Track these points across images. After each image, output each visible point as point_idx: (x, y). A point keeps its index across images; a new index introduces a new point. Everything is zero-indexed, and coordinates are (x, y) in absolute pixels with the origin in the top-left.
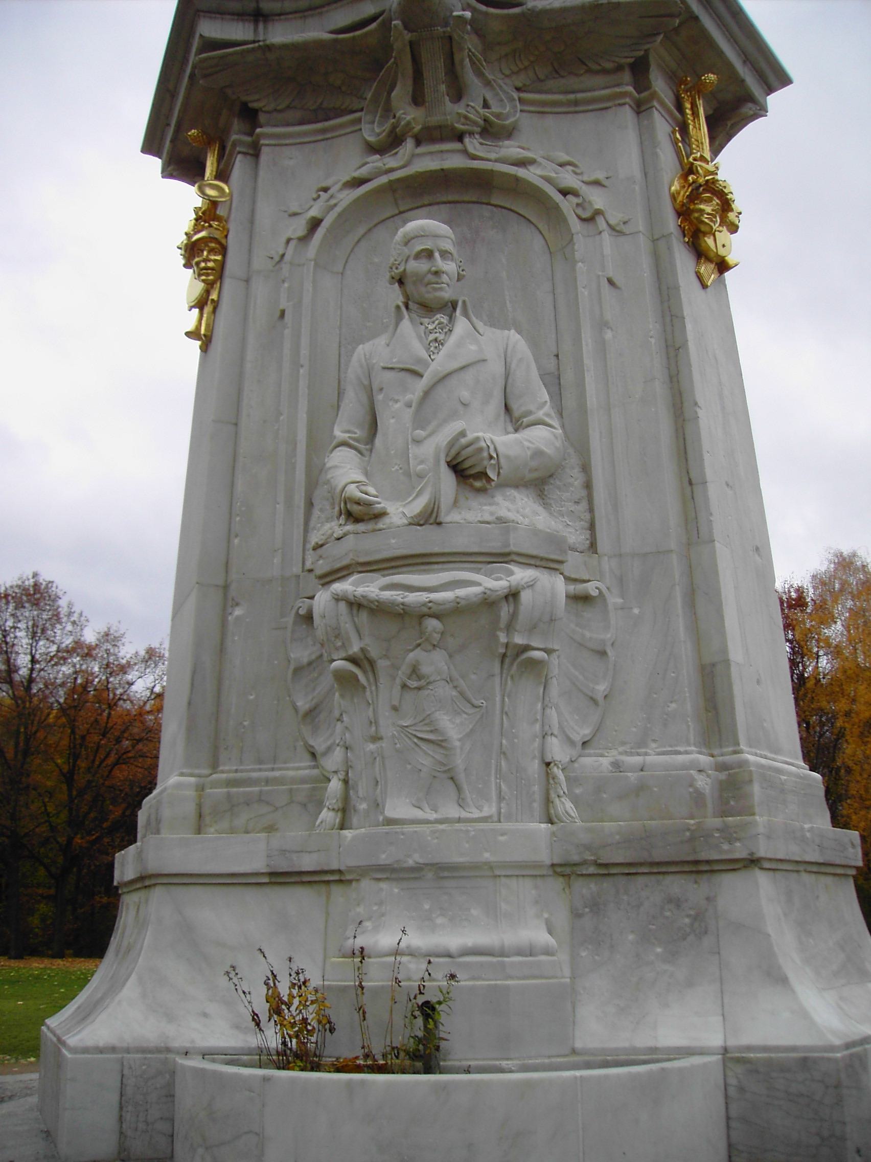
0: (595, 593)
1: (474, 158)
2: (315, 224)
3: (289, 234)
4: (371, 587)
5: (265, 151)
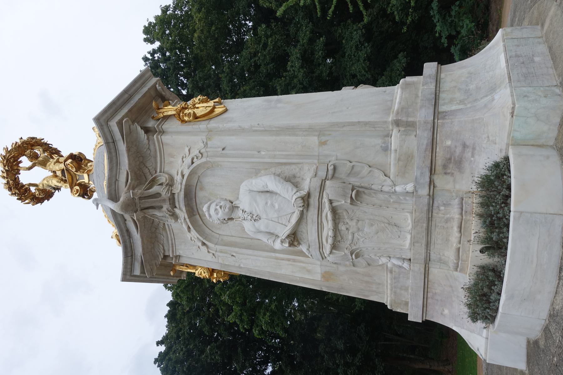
0: (332, 167)
1: (181, 190)
2: (204, 244)
3: (207, 251)
4: (327, 248)
5: (178, 254)
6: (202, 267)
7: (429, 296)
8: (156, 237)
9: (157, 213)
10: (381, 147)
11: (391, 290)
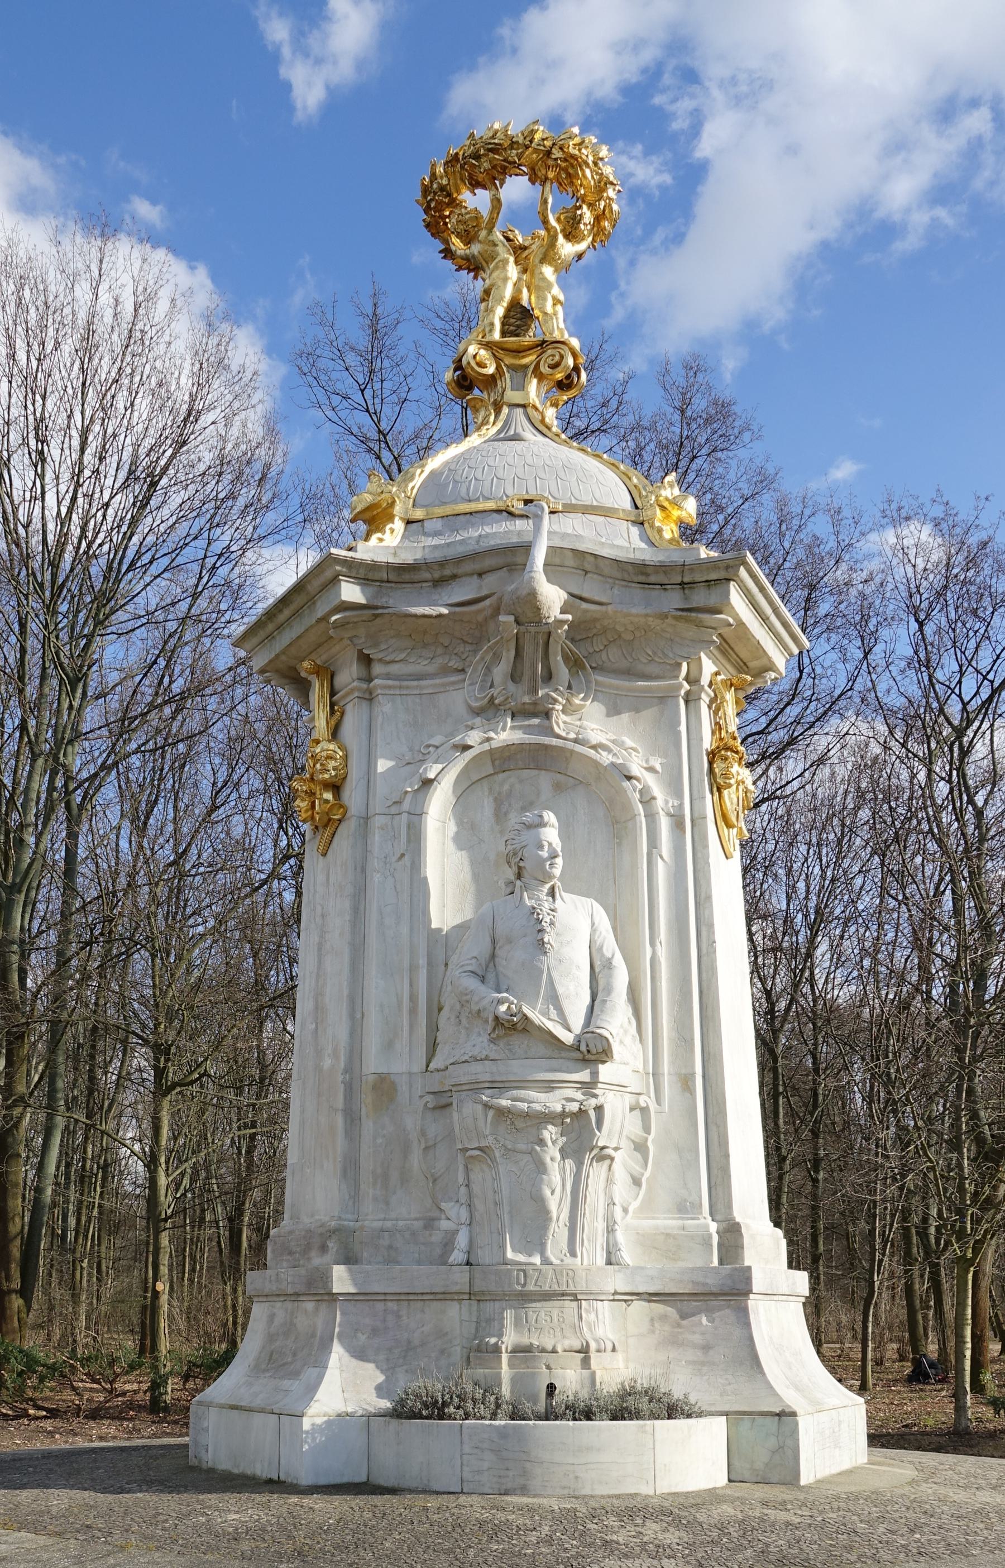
1: (558, 737)
6: (346, 758)
7: (389, 1304)
8: (425, 645)
9: (501, 671)
10: (685, 1201)
11: (382, 1230)
